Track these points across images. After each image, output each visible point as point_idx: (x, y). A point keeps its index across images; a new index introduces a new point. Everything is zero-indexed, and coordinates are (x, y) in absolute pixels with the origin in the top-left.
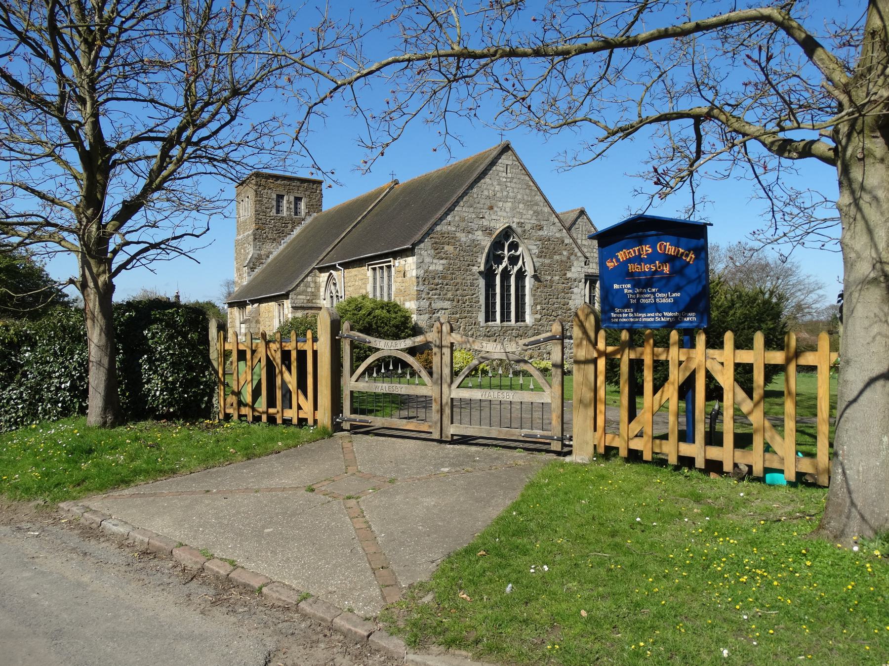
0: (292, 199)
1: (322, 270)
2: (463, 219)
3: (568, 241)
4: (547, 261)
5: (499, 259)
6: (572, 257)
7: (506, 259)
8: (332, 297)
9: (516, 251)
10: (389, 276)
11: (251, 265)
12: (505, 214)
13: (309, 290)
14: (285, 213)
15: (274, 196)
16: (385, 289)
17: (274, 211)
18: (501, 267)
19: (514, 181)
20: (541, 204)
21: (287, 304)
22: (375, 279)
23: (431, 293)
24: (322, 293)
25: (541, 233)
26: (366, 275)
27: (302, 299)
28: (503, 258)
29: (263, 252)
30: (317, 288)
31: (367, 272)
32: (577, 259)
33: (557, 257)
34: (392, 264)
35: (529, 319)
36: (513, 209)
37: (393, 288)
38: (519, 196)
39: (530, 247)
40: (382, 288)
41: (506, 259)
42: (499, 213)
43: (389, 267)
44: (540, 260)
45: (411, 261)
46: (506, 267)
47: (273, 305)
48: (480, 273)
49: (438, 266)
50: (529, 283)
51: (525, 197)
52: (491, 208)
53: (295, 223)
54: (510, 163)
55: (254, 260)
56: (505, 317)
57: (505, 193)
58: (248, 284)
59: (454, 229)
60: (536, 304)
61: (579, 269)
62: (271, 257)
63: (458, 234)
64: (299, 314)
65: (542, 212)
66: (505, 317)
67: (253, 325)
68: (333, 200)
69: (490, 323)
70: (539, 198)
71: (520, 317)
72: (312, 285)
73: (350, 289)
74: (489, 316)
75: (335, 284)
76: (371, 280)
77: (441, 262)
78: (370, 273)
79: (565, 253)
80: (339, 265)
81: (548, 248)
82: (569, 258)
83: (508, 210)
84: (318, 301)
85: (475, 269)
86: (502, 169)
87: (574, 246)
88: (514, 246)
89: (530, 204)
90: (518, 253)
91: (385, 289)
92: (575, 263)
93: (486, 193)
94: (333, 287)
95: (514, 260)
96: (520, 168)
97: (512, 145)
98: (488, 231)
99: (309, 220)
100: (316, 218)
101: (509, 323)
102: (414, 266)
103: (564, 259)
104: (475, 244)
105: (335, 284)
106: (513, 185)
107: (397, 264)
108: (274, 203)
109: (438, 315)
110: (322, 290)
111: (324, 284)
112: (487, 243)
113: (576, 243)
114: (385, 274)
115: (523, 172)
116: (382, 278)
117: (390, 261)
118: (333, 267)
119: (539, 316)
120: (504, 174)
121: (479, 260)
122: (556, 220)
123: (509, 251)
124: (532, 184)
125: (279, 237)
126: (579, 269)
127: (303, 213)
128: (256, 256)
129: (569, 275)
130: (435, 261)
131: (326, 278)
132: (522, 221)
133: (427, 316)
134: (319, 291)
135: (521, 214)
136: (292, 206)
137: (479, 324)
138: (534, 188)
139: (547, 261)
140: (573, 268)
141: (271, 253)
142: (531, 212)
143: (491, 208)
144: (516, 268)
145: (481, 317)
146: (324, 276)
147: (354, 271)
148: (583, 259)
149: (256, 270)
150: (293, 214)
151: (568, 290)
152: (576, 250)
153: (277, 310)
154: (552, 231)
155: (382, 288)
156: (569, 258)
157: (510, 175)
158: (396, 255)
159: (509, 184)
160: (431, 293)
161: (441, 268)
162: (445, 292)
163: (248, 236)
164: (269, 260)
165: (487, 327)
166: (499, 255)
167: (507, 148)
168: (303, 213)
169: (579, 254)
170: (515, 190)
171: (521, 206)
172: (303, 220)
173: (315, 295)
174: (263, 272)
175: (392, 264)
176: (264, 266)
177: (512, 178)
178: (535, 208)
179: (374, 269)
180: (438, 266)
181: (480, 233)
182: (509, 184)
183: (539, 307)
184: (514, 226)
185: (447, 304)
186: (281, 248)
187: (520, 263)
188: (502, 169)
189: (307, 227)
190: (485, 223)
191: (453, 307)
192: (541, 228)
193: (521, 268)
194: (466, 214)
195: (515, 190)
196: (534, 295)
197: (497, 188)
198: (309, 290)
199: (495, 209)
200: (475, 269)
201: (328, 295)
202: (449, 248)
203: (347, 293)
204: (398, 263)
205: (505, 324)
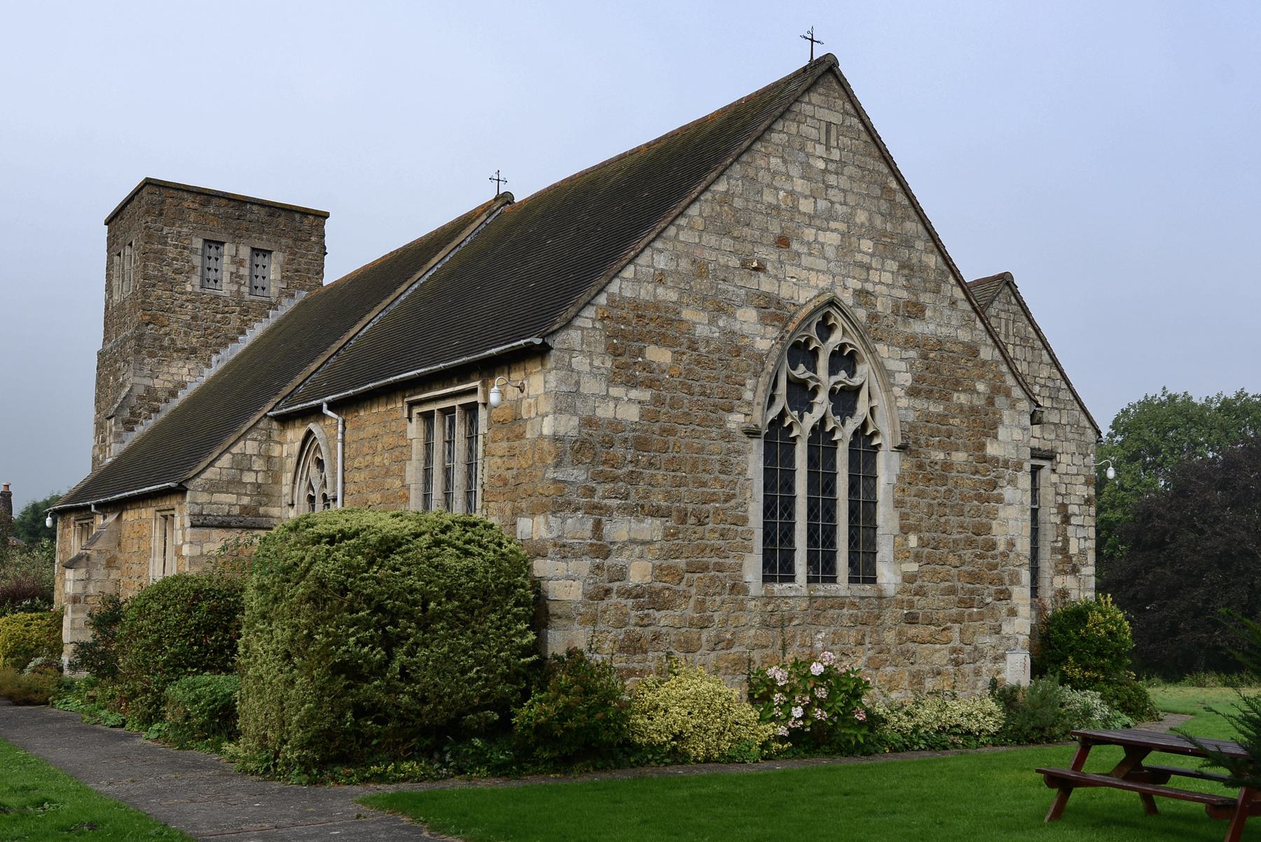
0: (245, 252)
1: (285, 420)
2: (701, 269)
3: (988, 353)
4: (936, 408)
5: (802, 394)
6: (1000, 401)
7: (822, 396)
8: (311, 499)
9: (852, 374)
10: (471, 438)
11: (126, 414)
12: (822, 264)
13: (249, 478)
14: (226, 289)
15: (198, 243)
16: (459, 477)
17: (196, 280)
18: (810, 420)
19: (849, 170)
20: (920, 245)
21: (182, 514)
22: (428, 446)
23: (600, 490)
24: (286, 489)
25: (917, 327)
26: (403, 434)
27: (227, 501)
28: (815, 392)
29: (158, 384)
30: (272, 468)
31: (399, 428)
32: (1013, 407)
33: (961, 398)
34: (479, 398)
35: (888, 575)
36: (845, 249)
37: (482, 476)
38: (861, 217)
39: (892, 365)
40: (447, 472)
41: (822, 396)
42: (805, 261)
43: (471, 409)
44: (920, 404)
45: (537, 383)
46: (823, 420)
47: (147, 513)
48: (751, 433)
49: (626, 407)
50: (888, 468)
51: (878, 221)
52: (783, 242)
53: (250, 312)
54: (835, 118)
55: (134, 401)
56: (822, 568)
57: (822, 204)
58: (112, 464)
59: (673, 296)
60: (905, 530)
61: (1017, 435)
62: (183, 395)
63: (687, 314)
64: (216, 541)
65: (924, 268)
66: (822, 568)
67: (100, 573)
68: (344, 257)
69: (777, 588)
70: (912, 227)
71: (863, 571)
72: (258, 464)
73: (359, 477)
74: (777, 565)
75: (320, 463)
76: (417, 448)
77: (634, 394)
78: (415, 430)
79: (981, 387)
80: (332, 406)
81: (937, 374)
82: (990, 401)
83: (830, 253)
84: (275, 511)
85: (735, 421)
86: (813, 133)
87: (1004, 368)
88: (844, 360)
89: (888, 245)
90: (856, 381)
91: (459, 477)
92: (1007, 416)
93: (768, 197)
94: (314, 470)
95: (845, 399)
96: (864, 136)
97: (845, 68)
98: (772, 310)
99: (287, 306)
100: (304, 303)
101: (831, 587)
102: (545, 406)
103: (979, 402)
104: (734, 347)
105: (320, 463)
106: (844, 182)
107: (494, 398)
108: (197, 260)
109: (621, 560)
110: (287, 478)
111: (291, 463)
112: (765, 341)
113: (1008, 361)
114: (460, 430)
115: (874, 150)
116: (450, 442)
117: (474, 391)
118: (316, 413)
119: (913, 567)
120: (820, 150)
121: (748, 395)
122: (958, 293)
123: (833, 371)
124: (894, 185)
125: (206, 345)
126: (1017, 435)
127: (273, 291)
128: (140, 391)
129: (992, 449)
130: (616, 391)
131: (297, 445)
132: (869, 287)
133: (585, 565)
134: (277, 480)
135: (868, 268)
136: (244, 271)
137: (745, 591)
138: (900, 198)
139: (936, 408)
140: (1002, 433)
141: (183, 385)
142: (892, 265)
143: (783, 242)
144: (852, 425)
145: (752, 569)
146: (295, 435)
147: (370, 416)
148: (1025, 405)
149: (141, 430)
150: (245, 289)
151: (989, 494)
152: (1010, 381)
153: (158, 534)
154: (944, 323)
155: (447, 472)
156: (990, 401)
157: (836, 155)
158: (489, 368)
159: (832, 179)
160: (600, 490)
161: (631, 414)
162: (642, 486)
163: (126, 340)
164: (175, 403)
165: (770, 598)
166: (803, 384)
167: (823, 73)
168: (273, 291)
169: (1017, 392)
170: (851, 199)
171: (867, 245)
172: (273, 306)
173: (264, 493)
174: (153, 432)
175: (479, 398)
176: (162, 416)
177: (842, 163)
178: (905, 253)
179: (428, 417)
180: (626, 407)
181: (747, 318)
182: (832, 179)
183: (913, 541)
184: (847, 299)
185: (651, 528)
186: (209, 373)
187: (862, 407)
188: (813, 133)
189: (279, 324)
190: (766, 284)
191: (668, 536)
192: (915, 311)
193: (865, 425)
194: (708, 255)
195: (851, 199)
196: (898, 504)
197: (800, 185)
198: (249, 478)
199: (795, 246)
200: (735, 421)
201: (301, 494)
202: (659, 355)
203: (351, 488)
204: (496, 393)
205: (822, 589)
